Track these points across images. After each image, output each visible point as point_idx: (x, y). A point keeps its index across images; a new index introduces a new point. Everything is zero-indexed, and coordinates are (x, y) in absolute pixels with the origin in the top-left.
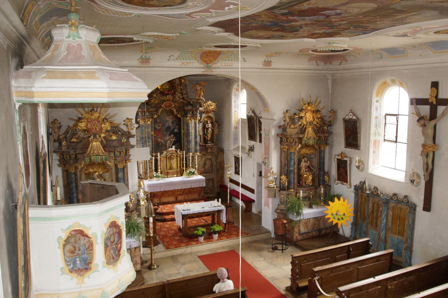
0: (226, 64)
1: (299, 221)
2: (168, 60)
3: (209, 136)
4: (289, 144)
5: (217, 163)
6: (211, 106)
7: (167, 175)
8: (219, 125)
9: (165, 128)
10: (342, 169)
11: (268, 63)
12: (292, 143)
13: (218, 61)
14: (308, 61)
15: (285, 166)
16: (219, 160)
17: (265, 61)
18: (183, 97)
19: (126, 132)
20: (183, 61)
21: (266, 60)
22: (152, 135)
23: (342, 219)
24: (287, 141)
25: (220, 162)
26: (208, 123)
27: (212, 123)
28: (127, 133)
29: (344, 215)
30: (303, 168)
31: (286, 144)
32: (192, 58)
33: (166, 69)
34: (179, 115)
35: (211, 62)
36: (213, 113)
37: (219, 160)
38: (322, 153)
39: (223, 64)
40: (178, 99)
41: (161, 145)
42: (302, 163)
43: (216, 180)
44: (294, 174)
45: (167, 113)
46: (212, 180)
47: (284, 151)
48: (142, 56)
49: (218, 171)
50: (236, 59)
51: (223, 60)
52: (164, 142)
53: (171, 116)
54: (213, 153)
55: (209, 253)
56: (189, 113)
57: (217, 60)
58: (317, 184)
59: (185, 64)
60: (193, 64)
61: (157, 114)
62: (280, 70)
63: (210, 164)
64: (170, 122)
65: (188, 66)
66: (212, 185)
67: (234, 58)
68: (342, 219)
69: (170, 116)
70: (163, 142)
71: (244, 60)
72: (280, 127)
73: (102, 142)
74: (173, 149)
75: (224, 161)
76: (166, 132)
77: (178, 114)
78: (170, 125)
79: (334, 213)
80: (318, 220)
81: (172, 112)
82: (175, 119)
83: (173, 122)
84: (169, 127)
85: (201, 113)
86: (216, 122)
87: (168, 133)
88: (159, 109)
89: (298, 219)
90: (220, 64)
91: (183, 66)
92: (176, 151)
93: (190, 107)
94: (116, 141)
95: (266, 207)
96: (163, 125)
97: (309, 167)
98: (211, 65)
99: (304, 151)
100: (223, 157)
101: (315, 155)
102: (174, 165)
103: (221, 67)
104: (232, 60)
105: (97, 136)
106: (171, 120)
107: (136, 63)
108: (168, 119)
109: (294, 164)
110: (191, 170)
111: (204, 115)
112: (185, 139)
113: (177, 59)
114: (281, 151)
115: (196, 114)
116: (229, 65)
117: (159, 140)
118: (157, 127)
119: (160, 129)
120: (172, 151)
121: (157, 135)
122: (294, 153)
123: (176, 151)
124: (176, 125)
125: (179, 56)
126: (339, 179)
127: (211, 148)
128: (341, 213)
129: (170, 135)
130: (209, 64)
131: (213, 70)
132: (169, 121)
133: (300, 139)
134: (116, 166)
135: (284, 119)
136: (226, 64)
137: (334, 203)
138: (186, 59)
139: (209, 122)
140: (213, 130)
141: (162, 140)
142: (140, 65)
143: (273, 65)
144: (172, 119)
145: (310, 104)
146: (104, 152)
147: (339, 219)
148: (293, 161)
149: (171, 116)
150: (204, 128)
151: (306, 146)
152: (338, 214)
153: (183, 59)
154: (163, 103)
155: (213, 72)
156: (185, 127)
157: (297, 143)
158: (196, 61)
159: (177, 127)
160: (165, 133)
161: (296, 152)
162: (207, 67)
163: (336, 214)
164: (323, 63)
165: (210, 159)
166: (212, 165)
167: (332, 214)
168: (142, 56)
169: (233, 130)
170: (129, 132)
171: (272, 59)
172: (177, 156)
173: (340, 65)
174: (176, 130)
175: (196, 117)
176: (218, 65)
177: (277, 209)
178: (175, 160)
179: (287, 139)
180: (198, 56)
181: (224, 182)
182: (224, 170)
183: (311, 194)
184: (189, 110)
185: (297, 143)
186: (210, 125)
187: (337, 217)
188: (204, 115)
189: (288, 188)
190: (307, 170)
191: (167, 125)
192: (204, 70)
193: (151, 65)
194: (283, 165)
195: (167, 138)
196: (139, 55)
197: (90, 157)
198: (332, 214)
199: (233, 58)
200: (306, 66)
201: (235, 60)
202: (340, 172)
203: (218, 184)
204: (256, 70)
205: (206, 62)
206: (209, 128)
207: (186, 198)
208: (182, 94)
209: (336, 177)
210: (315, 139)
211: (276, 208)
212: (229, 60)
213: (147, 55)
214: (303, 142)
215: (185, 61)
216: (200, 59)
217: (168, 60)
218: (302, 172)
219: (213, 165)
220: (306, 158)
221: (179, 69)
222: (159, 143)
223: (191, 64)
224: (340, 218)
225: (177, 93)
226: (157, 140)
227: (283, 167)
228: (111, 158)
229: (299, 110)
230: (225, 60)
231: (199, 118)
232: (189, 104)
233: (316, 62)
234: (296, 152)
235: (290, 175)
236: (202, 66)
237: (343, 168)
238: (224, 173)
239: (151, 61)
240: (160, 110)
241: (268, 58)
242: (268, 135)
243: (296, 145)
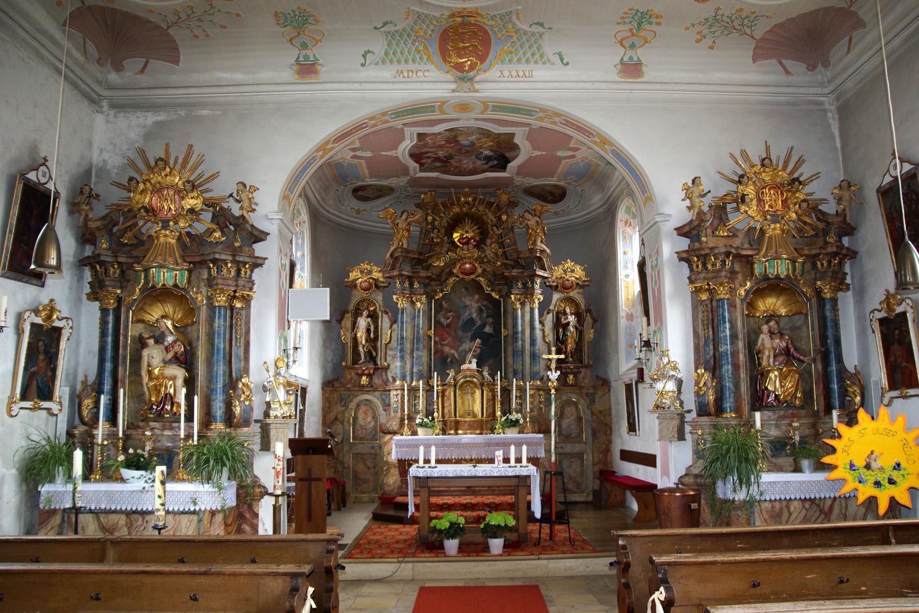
0: (514, 73)
1: (750, 504)
2: (363, 65)
3: (570, 345)
4: (710, 275)
5: (593, 414)
6: (573, 271)
7: (456, 430)
8: (595, 321)
9: (460, 323)
10: (896, 347)
11: (632, 69)
12: (720, 271)
13: (490, 66)
14: (754, 60)
15: (706, 344)
16: (598, 406)
17: (622, 62)
18: (505, 252)
19: (238, 218)
20: (400, 67)
21: (626, 59)
22: (431, 337)
24: (706, 268)
25: (601, 412)
26: (565, 314)
27: (578, 314)
28: (241, 221)
30: (767, 353)
31: (702, 275)
32: (421, 59)
33: (357, 86)
34: (493, 294)
35: (472, 67)
36: (581, 290)
37: (598, 406)
38: (828, 306)
39: (506, 73)
40: (492, 255)
41: (452, 362)
42: (762, 336)
43: (588, 458)
44: (736, 367)
45: (466, 289)
46: (580, 456)
47: (702, 302)
48: (298, 57)
49: (594, 434)
50: (537, 56)
51: (503, 62)
52: (460, 354)
53: (477, 297)
54: (581, 388)
55: (461, 584)
56: (514, 286)
57: (488, 61)
58: (822, 407)
59: (406, 74)
60: (426, 74)
61: (442, 291)
62: (671, 87)
63: (574, 417)
64: (473, 310)
65: (414, 78)
66: (579, 470)
67: (533, 55)
69: (472, 295)
70: (456, 355)
71: (562, 60)
72: (681, 231)
73: (179, 239)
74: (474, 366)
75: (610, 409)
76: (464, 331)
77: (492, 290)
78: (474, 316)
79: (860, 463)
80: (822, 512)
81: (478, 287)
82: (485, 303)
83: (480, 311)
84: (471, 321)
85: (549, 288)
86: (588, 311)
87: (469, 334)
88: (447, 279)
89: (741, 496)
90: (499, 74)
91: (402, 79)
92: (480, 373)
93: (515, 272)
94: (220, 247)
95: (665, 478)
96: (458, 317)
97: (787, 352)
98: (472, 74)
99: (771, 303)
100: (610, 400)
101: (806, 315)
102: (477, 408)
103: (502, 79)
104: (528, 61)
105: (171, 223)
106: (475, 305)
107: (288, 74)
108: (468, 303)
109: (734, 337)
110: (511, 417)
111: (556, 296)
112: (510, 349)
113: (383, 62)
114: (696, 304)
115: (533, 287)
116: (521, 74)
117: (447, 349)
118: (442, 320)
119: (449, 326)
120: (469, 370)
121: (443, 339)
122: (732, 305)
123: (480, 373)
124: (488, 316)
125: (386, 54)
126: (892, 387)
127: (575, 374)
129: (473, 339)
130: (468, 72)
131: (477, 86)
132: (472, 306)
133: (748, 262)
134: (210, 299)
135: (688, 203)
136: (514, 73)
137: (856, 429)
138: (406, 61)
139: (568, 311)
140: (580, 332)
141: (453, 351)
142: (295, 78)
143: (649, 73)
144: (477, 302)
145: (767, 161)
146: (179, 261)
148: (727, 325)
149: (477, 297)
150: (560, 325)
151: (771, 286)
152: (874, 465)
153: (399, 62)
154: (454, 264)
155: (477, 91)
156: (510, 321)
157: (740, 276)
158: (431, 67)
159: (490, 320)
160: (460, 333)
161: (738, 301)
162: (462, 79)
163: (868, 467)
164: (802, 67)
165: (576, 404)
166: (579, 419)
167: (852, 466)
168: (298, 57)
169: (623, 323)
170: (243, 216)
171: (642, 54)
172: (482, 385)
173: (848, 52)
174: (488, 329)
175: (532, 294)
176: (494, 73)
177: (686, 475)
178: (478, 393)
179: (704, 264)
180: (434, 49)
181: (611, 463)
182: (611, 434)
183: (795, 429)
184: (516, 279)
185: (740, 276)
186: (572, 319)
187: (870, 477)
188: (556, 296)
189: (719, 410)
190: (781, 359)
191: (465, 316)
192: (453, 86)
193: (322, 76)
194: (702, 343)
195: (465, 346)
196: (291, 55)
197: (146, 270)
199: (529, 54)
200: (752, 77)
201: (536, 62)
202: (892, 359)
203: (597, 468)
204: (597, 85)
205: (459, 67)
206: (568, 323)
208: (502, 245)
209: (885, 382)
210: (794, 261)
211: (683, 473)
212: (519, 61)
213: (308, 52)
214: (758, 269)
215: (403, 67)
216: (442, 61)
217: (363, 65)
218: (764, 363)
219: (581, 418)
220: (772, 323)
221: (390, 86)
222: (447, 357)
223: (420, 74)
225: (488, 241)
226: (442, 352)
227: (702, 350)
228: (202, 284)
229: (733, 181)
230: (510, 61)
231: (542, 298)
232: (517, 264)
233: (781, 63)
234: (738, 301)
235: (721, 367)
236: (449, 77)
237: (900, 343)
238: (610, 442)
239: (319, 67)
240: (451, 280)
241: (630, 53)
242: (656, 266)
243: (737, 282)
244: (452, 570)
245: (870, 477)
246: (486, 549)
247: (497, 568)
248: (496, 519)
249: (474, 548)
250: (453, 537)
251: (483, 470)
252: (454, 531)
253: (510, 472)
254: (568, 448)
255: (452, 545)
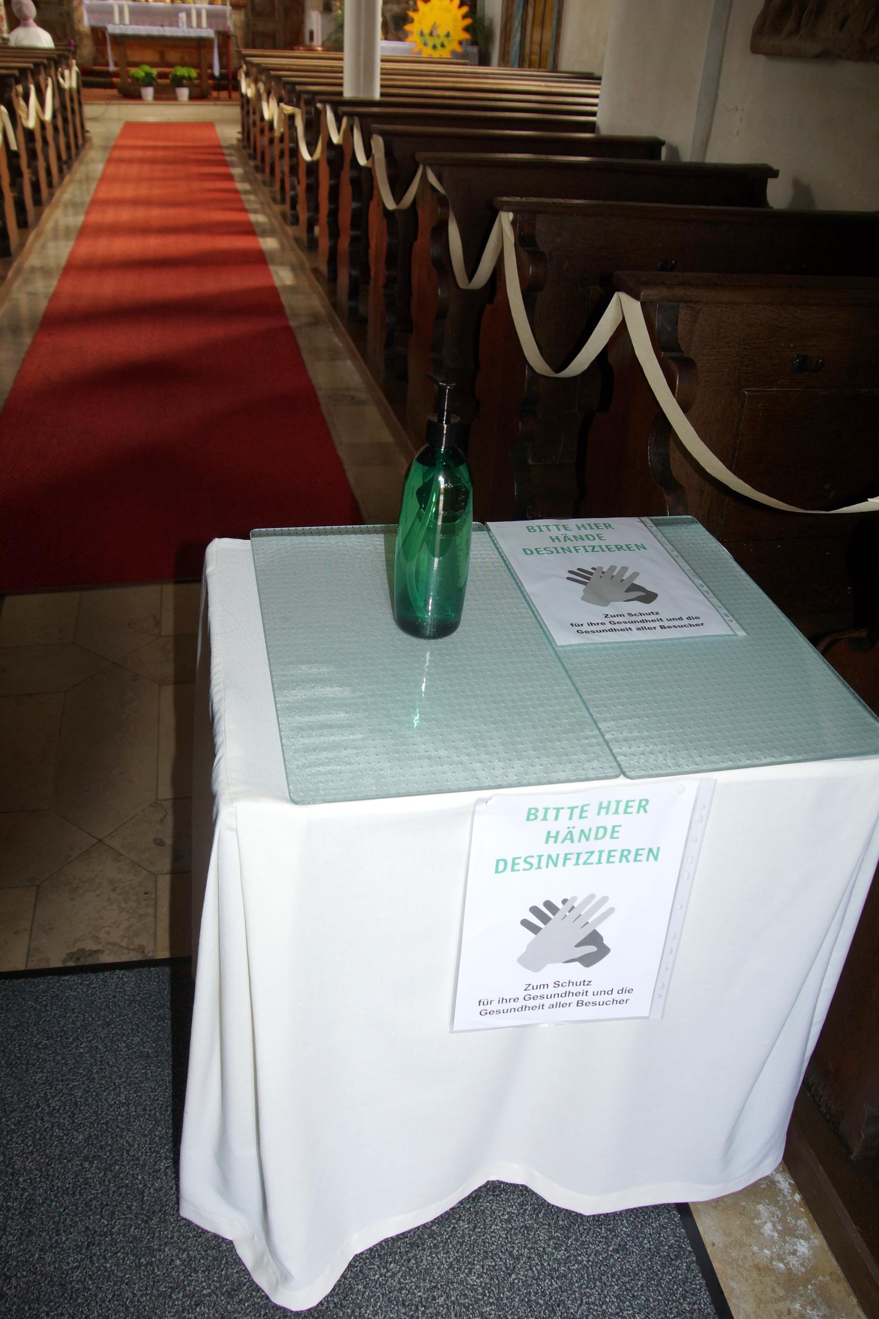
23: (443, 46)
29: (448, 35)
68: (443, 46)
79: (427, 31)
128: (442, 32)
147: (434, 47)
152: (435, 33)
163: (431, 34)
167: (422, 34)
187: (431, 41)
198: (422, 34)
207: (187, 58)
224: (438, 43)
244: (149, 111)
245: (431, 41)
246: (174, 98)
247: (183, 110)
248: (181, 71)
249: (166, 94)
250: (148, 84)
251: (168, 31)
252: (148, 81)
253: (194, 33)
254: (261, 27)
255: (148, 93)
